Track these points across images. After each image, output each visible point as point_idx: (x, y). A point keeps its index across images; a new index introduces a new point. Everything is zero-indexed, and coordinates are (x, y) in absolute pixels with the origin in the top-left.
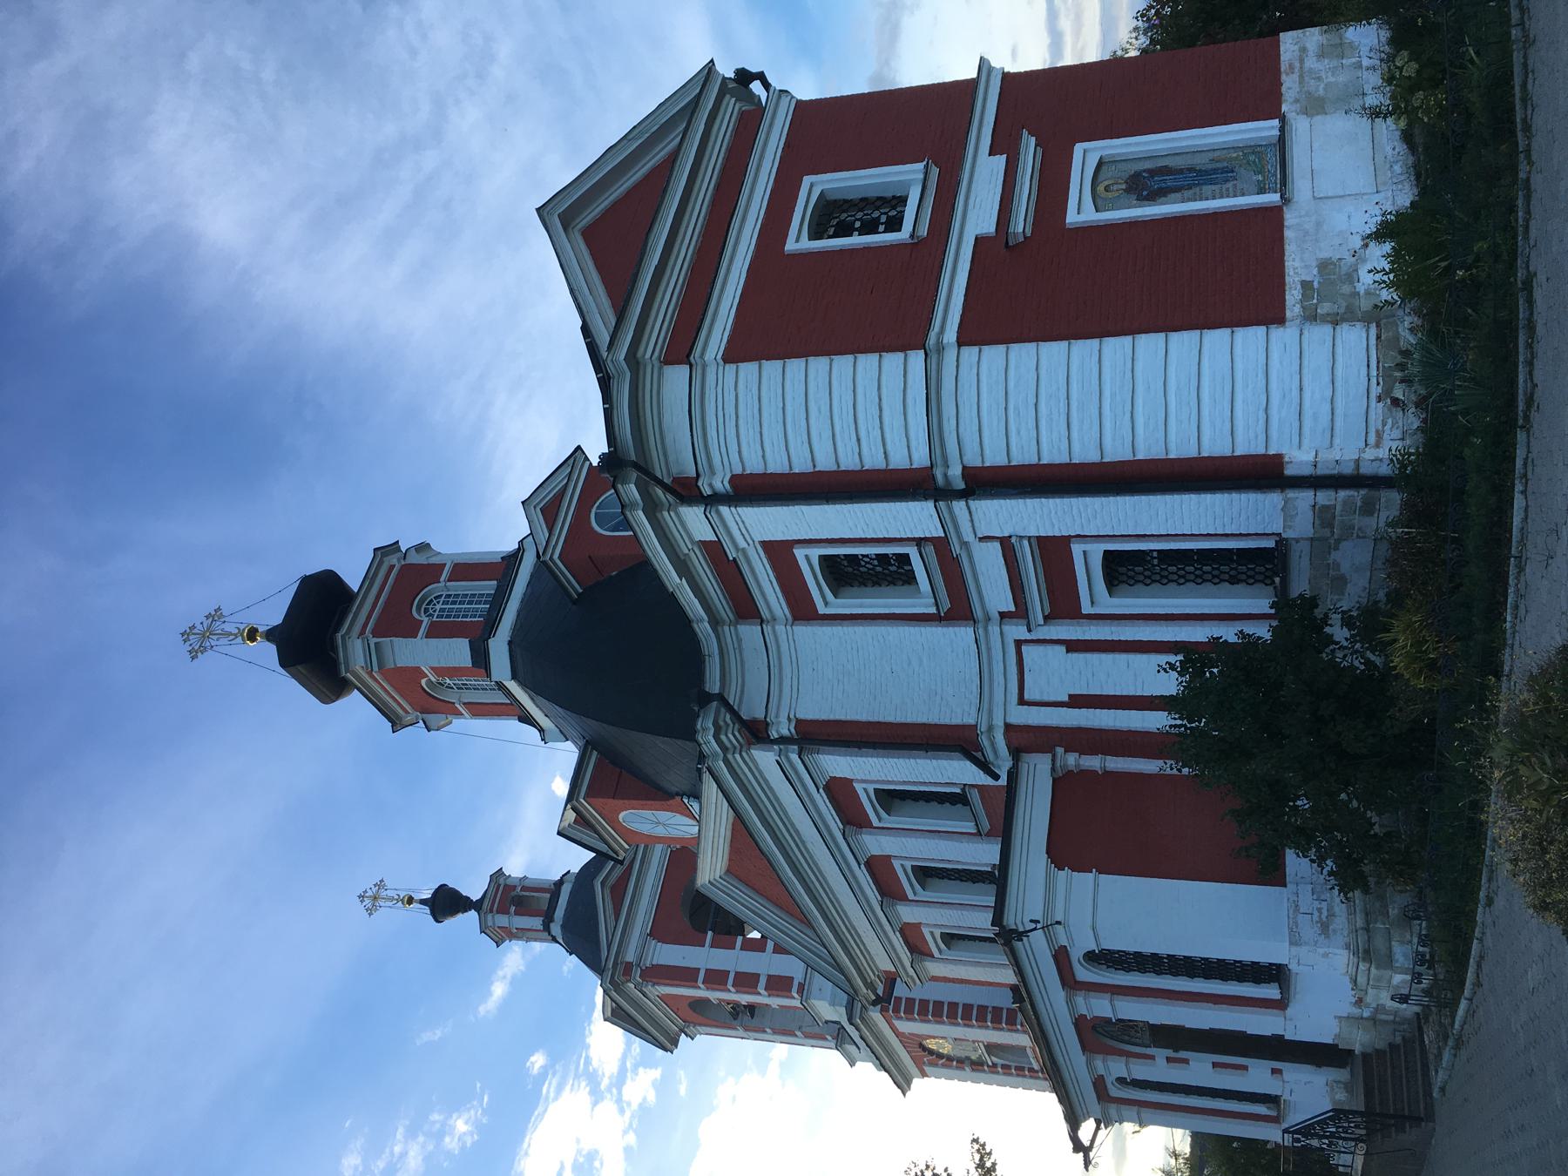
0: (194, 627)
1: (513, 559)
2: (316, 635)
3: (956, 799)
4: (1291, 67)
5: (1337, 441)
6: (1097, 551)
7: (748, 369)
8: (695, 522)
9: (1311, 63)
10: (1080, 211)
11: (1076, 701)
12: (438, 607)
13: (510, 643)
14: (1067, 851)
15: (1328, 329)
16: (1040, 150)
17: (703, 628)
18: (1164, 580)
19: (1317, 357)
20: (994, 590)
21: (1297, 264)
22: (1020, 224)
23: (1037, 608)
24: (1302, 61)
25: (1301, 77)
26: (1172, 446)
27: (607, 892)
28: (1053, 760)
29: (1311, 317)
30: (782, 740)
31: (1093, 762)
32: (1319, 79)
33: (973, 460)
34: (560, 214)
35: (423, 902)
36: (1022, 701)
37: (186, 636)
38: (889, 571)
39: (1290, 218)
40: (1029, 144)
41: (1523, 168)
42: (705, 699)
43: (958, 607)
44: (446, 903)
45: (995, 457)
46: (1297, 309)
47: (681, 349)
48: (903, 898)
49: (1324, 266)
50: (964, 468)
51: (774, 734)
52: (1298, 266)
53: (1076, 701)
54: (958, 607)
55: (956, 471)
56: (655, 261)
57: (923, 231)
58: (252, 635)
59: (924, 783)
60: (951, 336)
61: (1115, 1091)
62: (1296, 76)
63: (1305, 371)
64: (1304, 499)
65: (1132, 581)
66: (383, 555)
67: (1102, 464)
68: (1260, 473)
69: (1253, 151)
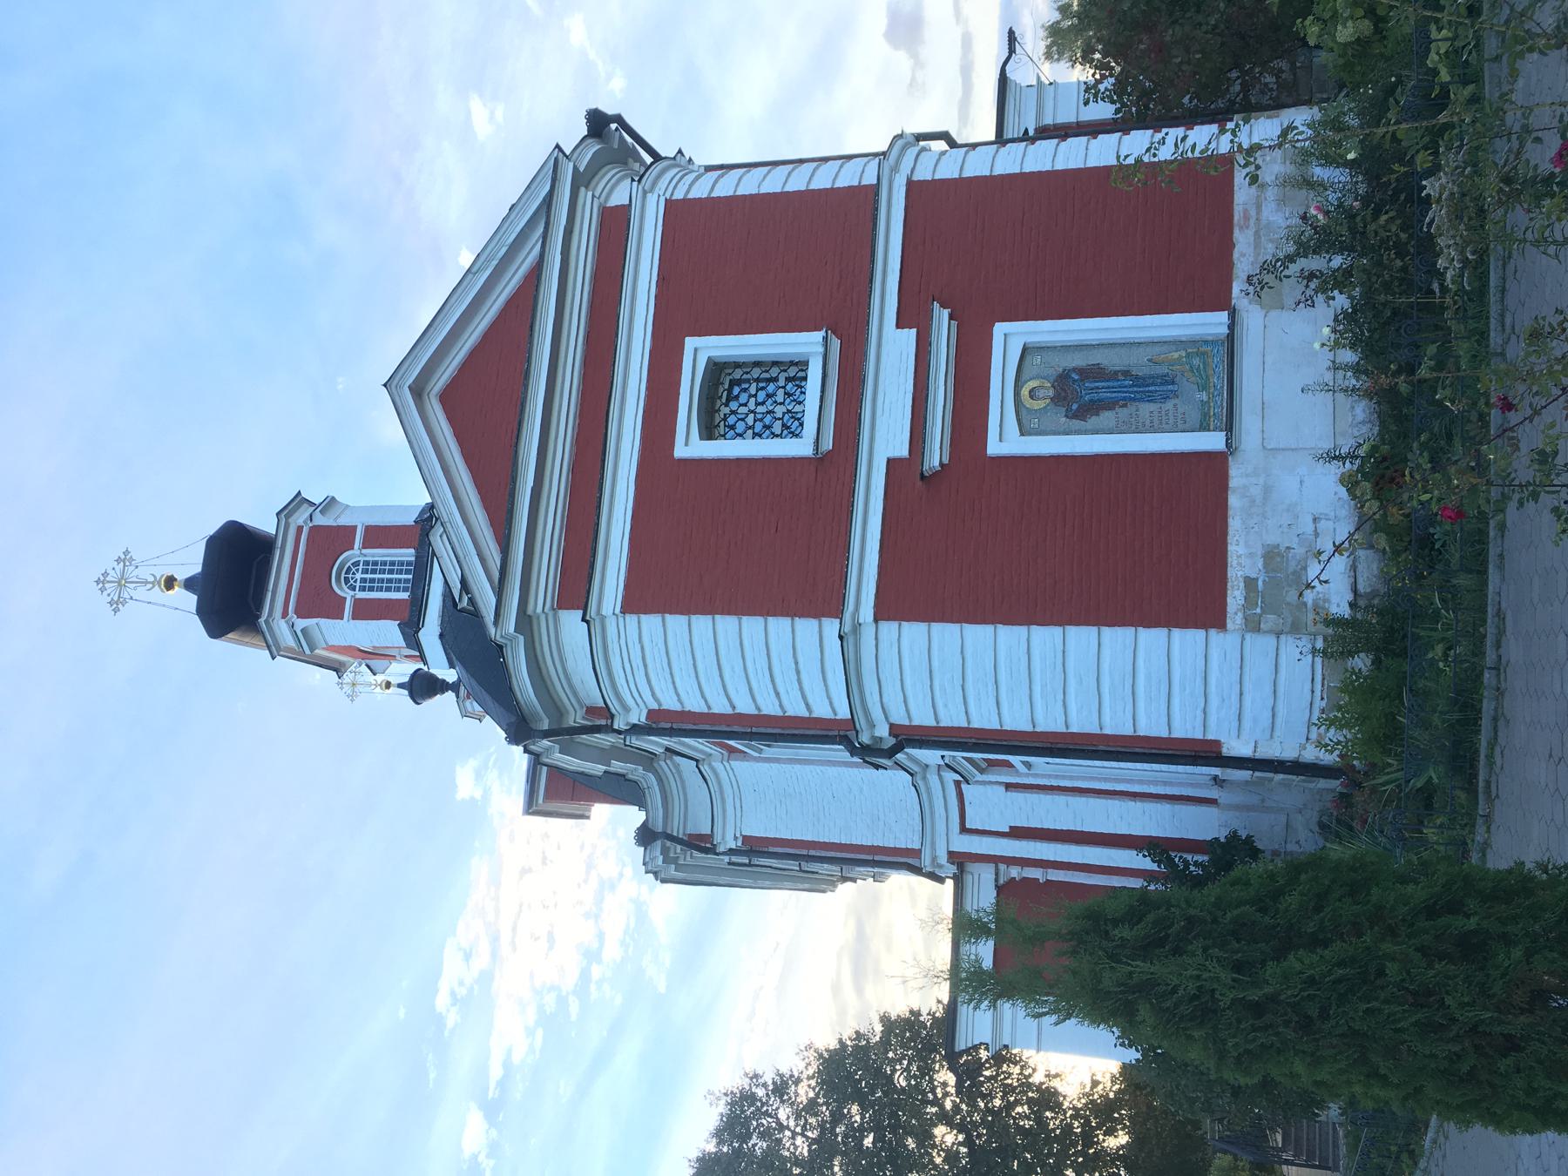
0: (105, 574)
4: (1246, 217)
5: (1277, 733)
7: (651, 622)
10: (1005, 439)
11: (1017, 833)
12: (359, 576)
13: (441, 636)
15: (1272, 640)
21: (1241, 550)
22: (935, 456)
24: (1259, 207)
25: (1257, 233)
26: (1107, 719)
28: (997, 874)
29: (1253, 625)
33: (899, 718)
35: (401, 686)
36: (964, 830)
37: (101, 582)
39: (1237, 476)
40: (942, 318)
41: (1481, 829)
46: (1239, 619)
47: (575, 589)
49: (1272, 556)
50: (892, 726)
51: (721, 849)
52: (1242, 558)
53: (1017, 833)
55: (883, 731)
57: (828, 444)
58: (170, 583)
59: (879, 345)
60: (867, 612)
62: (1250, 233)
63: (1246, 678)
66: (287, 517)
67: (1034, 734)
69: (1196, 347)
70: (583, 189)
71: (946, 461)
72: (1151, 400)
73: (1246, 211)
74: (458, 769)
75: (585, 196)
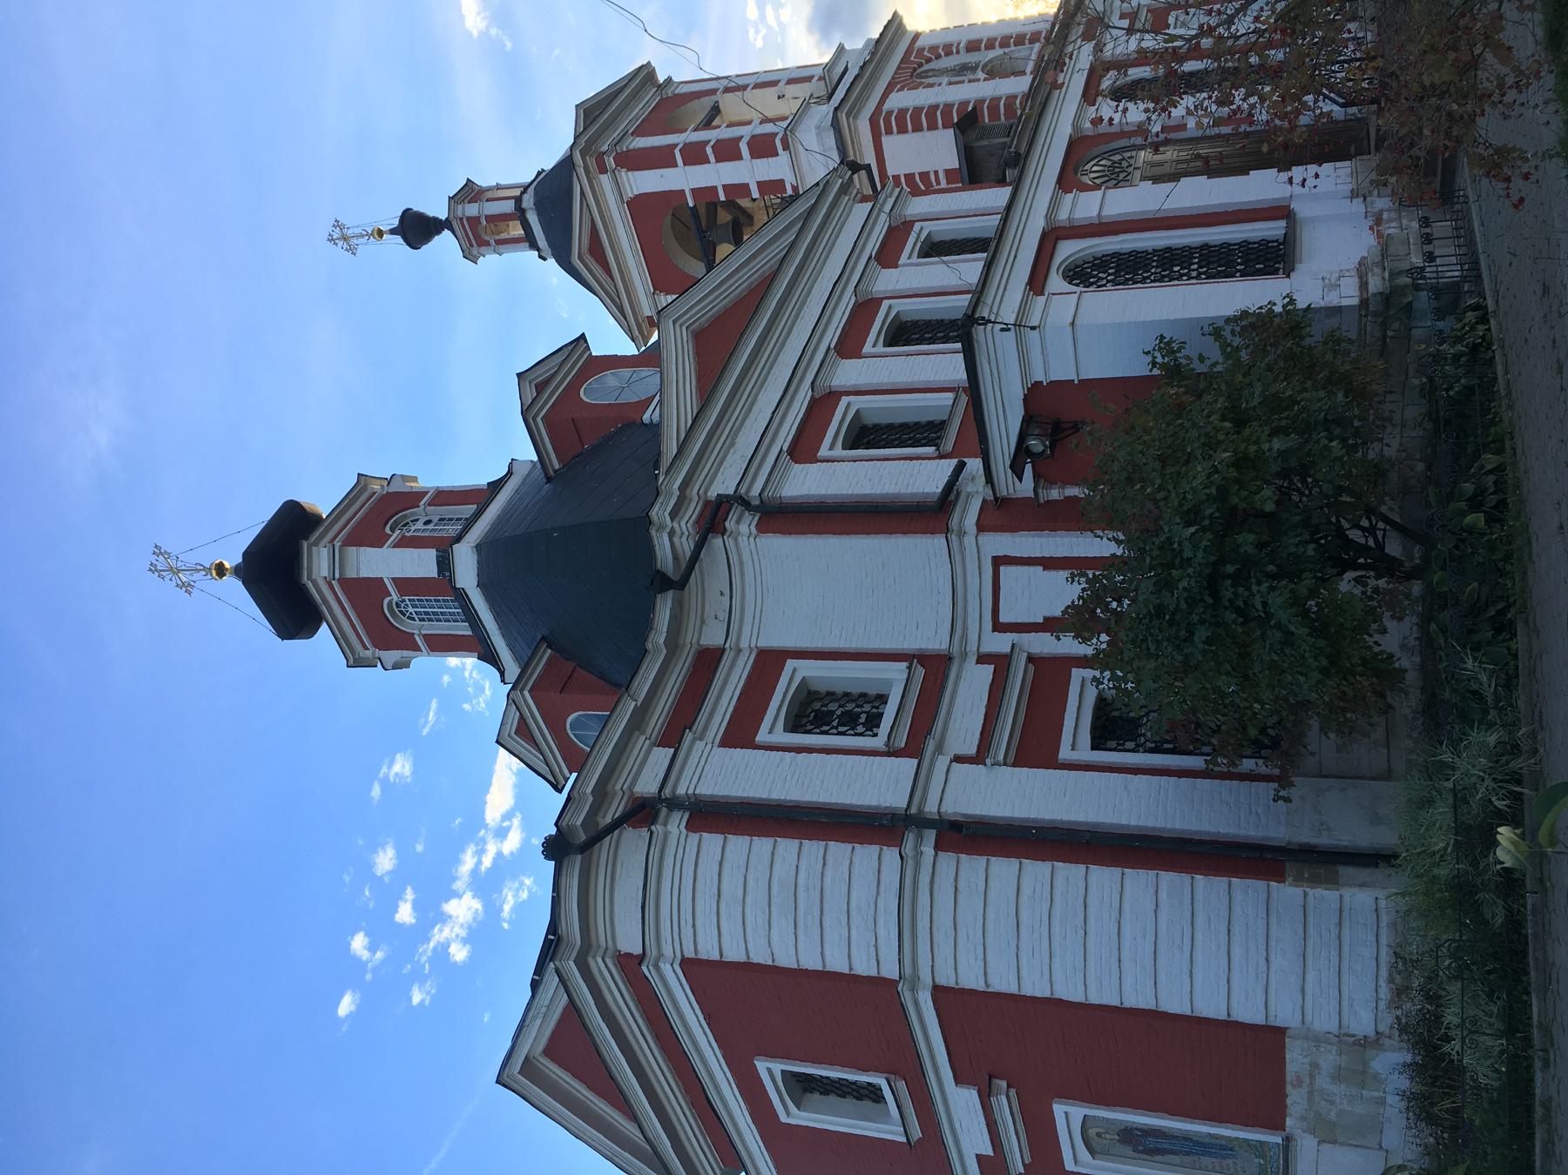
9: (1323, 1082)
12: (411, 609)
16: (1013, 1092)
24: (1312, 1077)
25: (1310, 1093)
27: (588, 258)
32: (1332, 1103)
34: (520, 1074)
35: (393, 232)
44: (416, 228)
56: (668, 1144)
57: (917, 1133)
62: (1305, 1090)
70: (590, 960)
71: (1028, 1160)
72: (1211, 1155)
73: (1298, 1078)
74: (527, 452)
75: (597, 964)
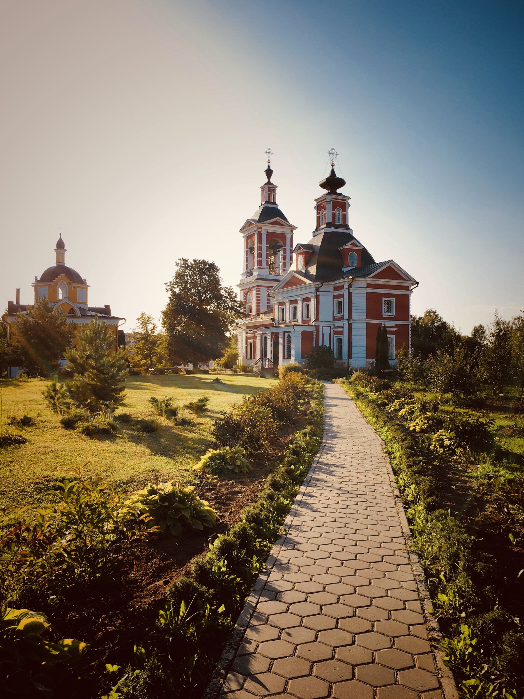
1: (347, 227)
2: (333, 183)
3: (308, 316)
6: (342, 338)
8: (346, 286)
11: (323, 334)
14: (304, 333)
17: (332, 283)
18: (338, 345)
19: (362, 362)
20: (337, 324)
23: (335, 330)
30: (316, 293)
31: (315, 336)
38: (340, 311)
40: (396, 329)
42: (322, 284)
43: (335, 319)
44: (269, 173)
45: (353, 327)
47: (369, 286)
48: (290, 304)
53: (323, 334)
54: (335, 319)
60: (368, 322)
61: (264, 336)
64: (347, 361)
65: (339, 342)
68: (350, 356)
